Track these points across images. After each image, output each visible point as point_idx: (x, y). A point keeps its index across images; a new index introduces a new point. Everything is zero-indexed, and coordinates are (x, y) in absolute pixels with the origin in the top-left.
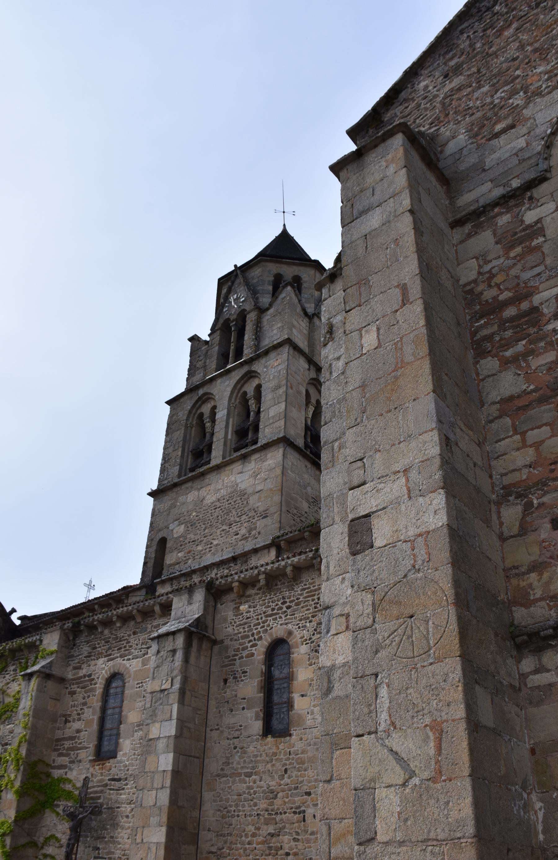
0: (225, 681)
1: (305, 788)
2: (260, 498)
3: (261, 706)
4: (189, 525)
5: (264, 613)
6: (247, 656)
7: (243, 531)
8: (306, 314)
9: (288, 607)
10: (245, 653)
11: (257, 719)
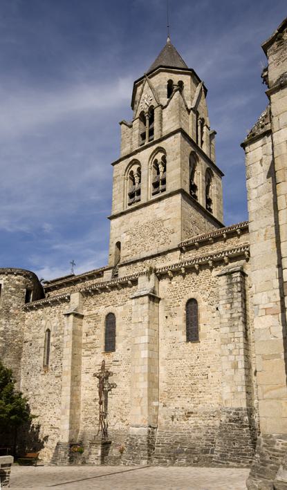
0: (167, 317)
1: (207, 365)
2: (170, 223)
3: (185, 329)
6: (177, 306)
7: (162, 240)
8: (187, 109)
10: (175, 305)
11: (183, 334)
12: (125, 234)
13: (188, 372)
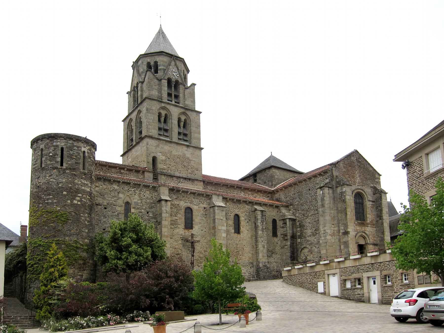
6: (229, 215)
9: (239, 208)
10: (229, 215)
12: (161, 154)
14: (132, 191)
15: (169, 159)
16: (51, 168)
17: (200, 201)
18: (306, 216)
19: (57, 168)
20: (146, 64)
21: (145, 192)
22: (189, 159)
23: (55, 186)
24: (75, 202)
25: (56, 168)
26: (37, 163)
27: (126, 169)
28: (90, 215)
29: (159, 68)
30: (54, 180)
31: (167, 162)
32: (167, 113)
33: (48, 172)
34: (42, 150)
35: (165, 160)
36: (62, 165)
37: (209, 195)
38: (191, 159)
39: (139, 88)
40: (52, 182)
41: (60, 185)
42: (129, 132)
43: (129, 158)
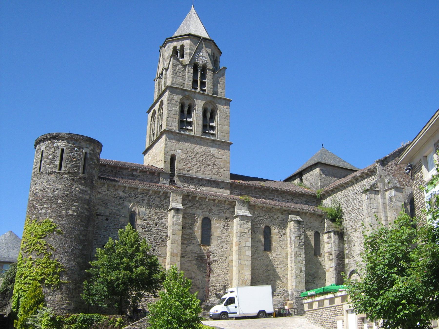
4: (188, 156)
5: (263, 217)
9: (270, 218)
13: (265, 268)
14: (140, 198)
15: (191, 157)
16: (48, 172)
17: (221, 209)
18: (353, 227)
19: (55, 173)
20: (172, 48)
21: (154, 199)
22: (214, 157)
23: (50, 194)
24: (70, 212)
25: (54, 173)
26: (36, 166)
27: (139, 171)
28: (87, 228)
29: (185, 52)
30: (50, 187)
31: (188, 160)
32: (192, 103)
33: (46, 177)
34: (42, 152)
35: (185, 159)
36: (60, 169)
37: (232, 202)
38: (216, 156)
39: (163, 75)
40: (48, 189)
41: (56, 193)
42: (152, 125)
43: (149, 156)
